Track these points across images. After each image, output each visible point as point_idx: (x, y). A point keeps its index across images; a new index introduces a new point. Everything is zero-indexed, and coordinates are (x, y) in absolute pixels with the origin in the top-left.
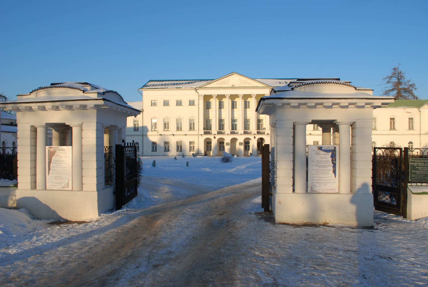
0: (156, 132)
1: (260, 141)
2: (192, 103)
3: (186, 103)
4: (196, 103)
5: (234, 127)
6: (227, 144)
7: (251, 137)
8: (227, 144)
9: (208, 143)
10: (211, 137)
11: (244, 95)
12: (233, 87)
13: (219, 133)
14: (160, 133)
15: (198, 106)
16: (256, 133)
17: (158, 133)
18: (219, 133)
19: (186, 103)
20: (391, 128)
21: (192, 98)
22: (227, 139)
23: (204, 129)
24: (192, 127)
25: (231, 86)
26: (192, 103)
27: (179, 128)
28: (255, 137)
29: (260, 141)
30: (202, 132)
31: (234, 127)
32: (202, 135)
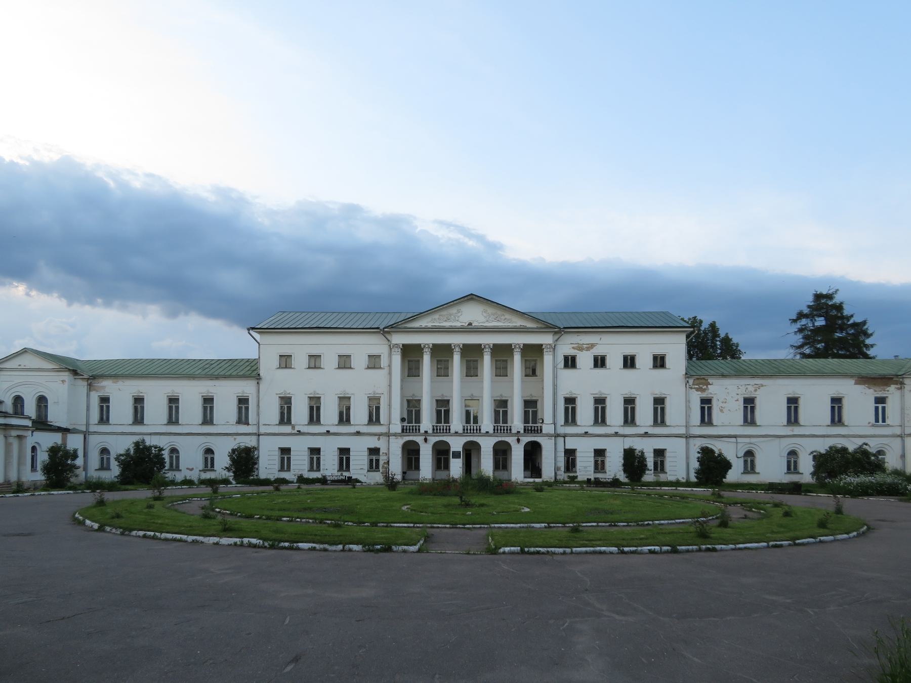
0: (290, 427)
1: (529, 448)
2: (374, 362)
3: (359, 361)
4: (384, 362)
5: (470, 418)
6: (456, 455)
7: (511, 440)
8: (456, 455)
9: (411, 454)
10: (419, 439)
11: (494, 345)
12: (470, 329)
13: (436, 431)
14: (297, 428)
16: (522, 431)
17: (293, 428)
18: (436, 431)
19: (359, 361)
20: (833, 421)
21: (375, 351)
22: (457, 444)
23: (403, 420)
24: (374, 417)
26: (374, 362)
27: (344, 418)
28: (518, 440)
29: (529, 448)
30: (397, 427)
31: (470, 418)
32: (395, 435)
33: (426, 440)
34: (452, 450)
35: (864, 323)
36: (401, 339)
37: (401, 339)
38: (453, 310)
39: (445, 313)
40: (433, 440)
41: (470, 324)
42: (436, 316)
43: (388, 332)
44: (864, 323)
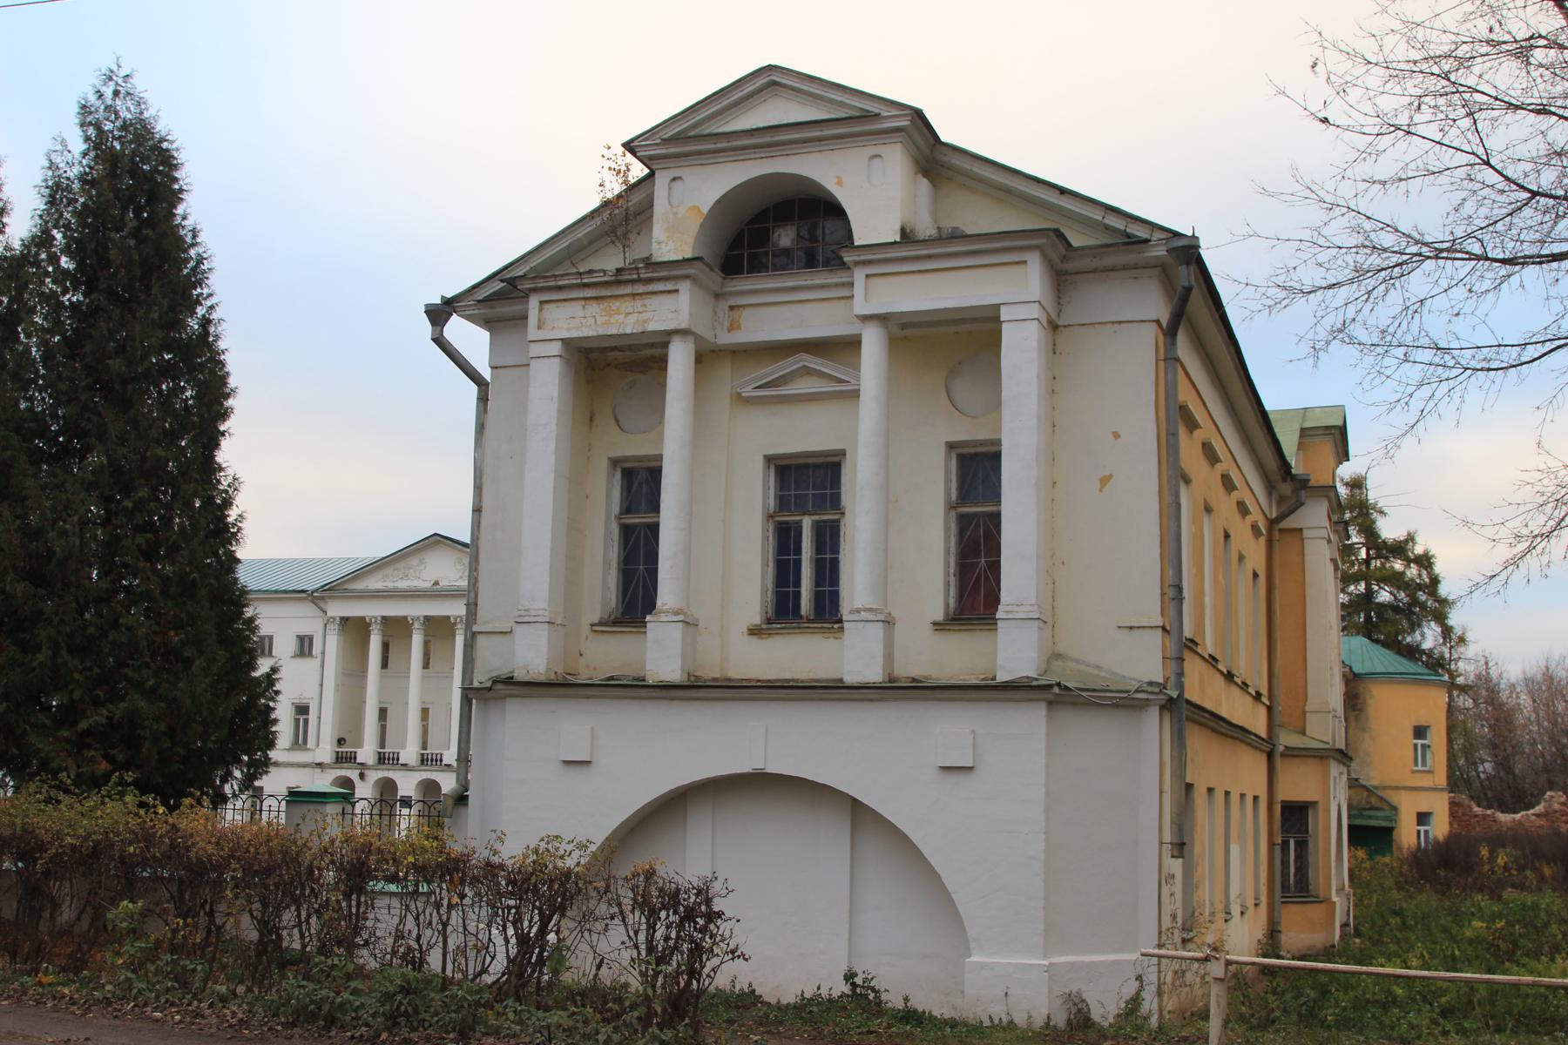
4: (317, 649)
10: (353, 774)
15: (318, 661)
18: (382, 759)
21: (305, 631)
22: (407, 785)
25: (428, 585)
26: (304, 647)
30: (325, 753)
32: (320, 765)
33: (362, 776)
34: (401, 793)
35: (1411, 538)
36: (338, 609)
37: (338, 609)
38: (414, 561)
39: (401, 565)
40: (374, 776)
41: (436, 583)
42: (389, 571)
43: (322, 598)
44: (1411, 538)
